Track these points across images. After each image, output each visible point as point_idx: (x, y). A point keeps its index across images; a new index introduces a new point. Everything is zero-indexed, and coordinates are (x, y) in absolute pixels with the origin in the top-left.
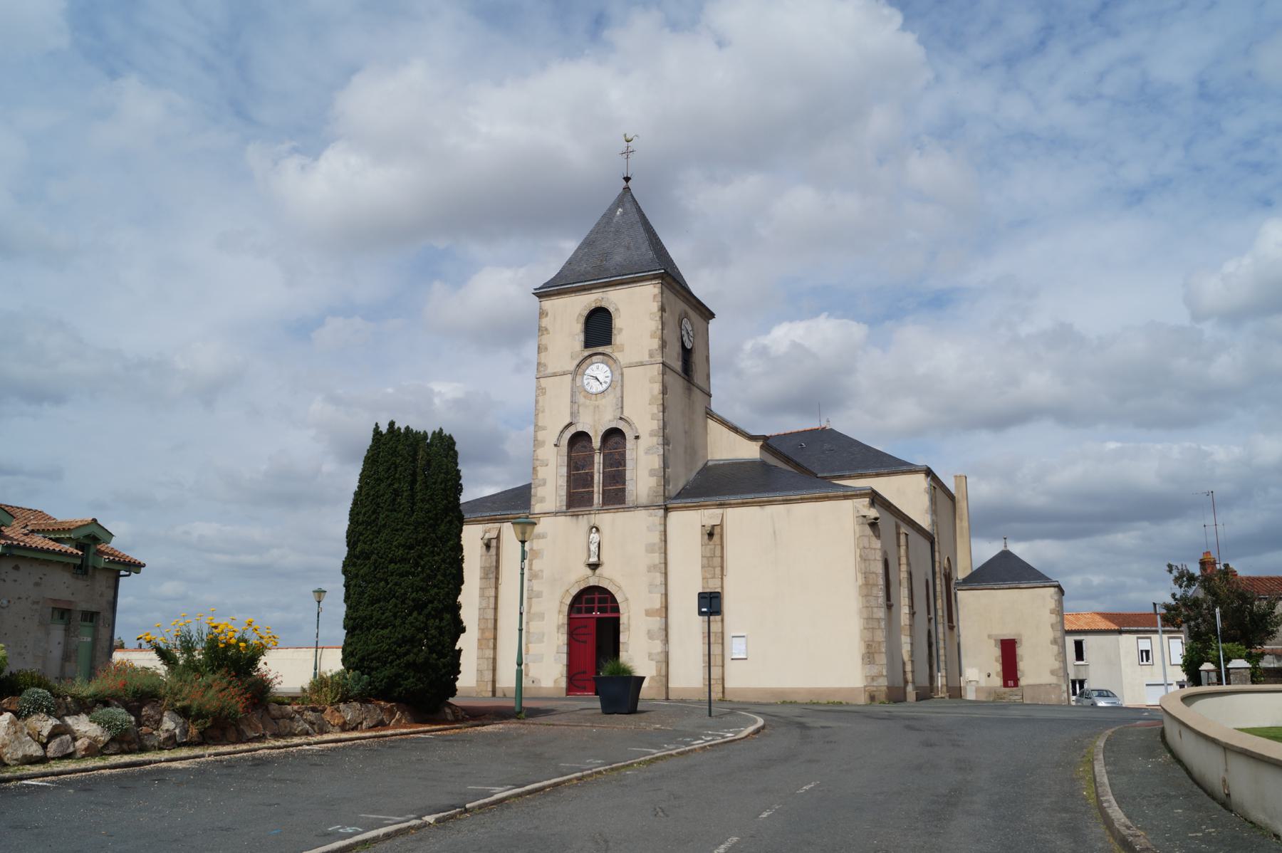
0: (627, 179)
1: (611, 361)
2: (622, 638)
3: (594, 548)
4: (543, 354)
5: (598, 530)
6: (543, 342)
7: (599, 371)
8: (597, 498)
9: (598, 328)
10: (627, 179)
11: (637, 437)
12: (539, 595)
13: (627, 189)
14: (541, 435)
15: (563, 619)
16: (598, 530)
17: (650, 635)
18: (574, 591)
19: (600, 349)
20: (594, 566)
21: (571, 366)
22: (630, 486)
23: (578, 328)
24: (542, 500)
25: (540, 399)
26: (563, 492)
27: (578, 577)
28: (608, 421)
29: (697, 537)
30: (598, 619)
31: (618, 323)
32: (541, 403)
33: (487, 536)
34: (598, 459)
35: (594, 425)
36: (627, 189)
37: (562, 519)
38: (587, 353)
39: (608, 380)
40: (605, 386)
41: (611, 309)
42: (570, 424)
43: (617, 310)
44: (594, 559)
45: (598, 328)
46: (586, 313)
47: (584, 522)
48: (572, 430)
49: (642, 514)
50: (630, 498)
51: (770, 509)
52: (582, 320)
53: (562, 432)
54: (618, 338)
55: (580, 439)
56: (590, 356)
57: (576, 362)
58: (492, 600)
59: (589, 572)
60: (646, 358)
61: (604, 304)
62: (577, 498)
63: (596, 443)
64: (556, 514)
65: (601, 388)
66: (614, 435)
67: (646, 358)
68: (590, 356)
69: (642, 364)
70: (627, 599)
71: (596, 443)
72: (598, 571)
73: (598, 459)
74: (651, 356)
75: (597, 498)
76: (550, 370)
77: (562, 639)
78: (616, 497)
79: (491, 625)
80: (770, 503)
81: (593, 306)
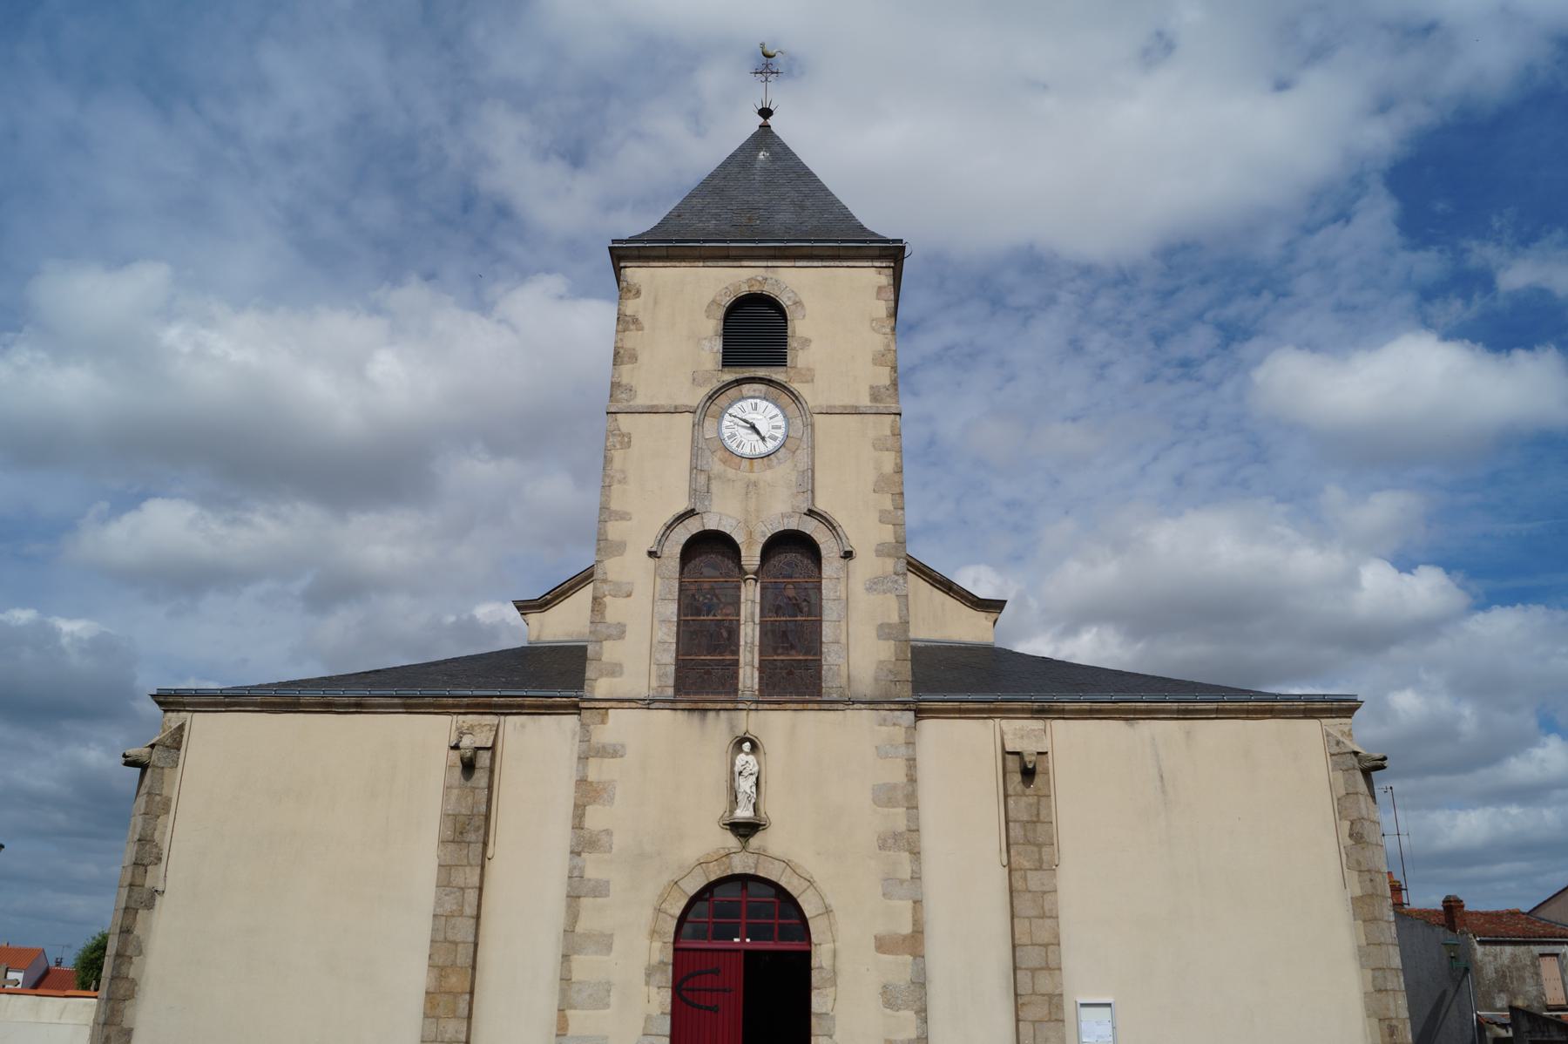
0: (766, 113)
1: (785, 399)
2: (818, 1003)
3: (746, 785)
4: (625, 369)
5: (755, 748)
6: (629, 344)
7: (755, 419)
8: (748, 677)
9: (755, 335)
10: (766, 113)
11: (848, 555)
12: (600, 890)
13: (765, 128)
14: (615, 530)
15: (661, 951)
16: (755, 748)
17: (890, 998)
18: (693, 886)
19: (761, 372)
20: (745, 830)
21: (697, 396)
22: (831, 657)
23: (712, 326)
24: (615, 670)
25: (617, 455)
26: (669, 658)
27: (702, 849)
28: (780, 513)
29: (986, 776)
30: (750, 955)
31: (799, 327)
32: (617, 464)
33: (467, 742)
34: (751, 594)
35: (751, 519)
36: (765, 128)
37: (663, 718)
38: (729, 376)
39: (780, 434)
40: (771, 445)
41: (785, 300)
42: (690, 513)
43: (797, 303)
44: (744, 813)
45: (755, 335)
46: (727, 301)
47: (719, 728)
48: (693, 527)
49: (863, 719)
50: (832, 683)
51: (1148, 729)
52: (721, 313)
53: (670, 527)
54: (799, 357)
55: (710, 546)
56: (739, 382)
57: (704, 391)
58: (472, 895)
59: (732, 841)
60: (865, 401)
61: (768, 289)
62: (701, 675)
63: (751, 557)
64: (649, 703)
65: (762, 449)
66: (793, 546)
67: (865, 401)
68: (739, 382)
69: (856, 412)
70: (828, 911)
71: (751, 557)
72: (755, 841)
73: (751, 594)
74: (875, 397)
75: (748, 677)
76: (641, 401)
77: (661, 999)
78: (796, 675)
79: (463, 958)
80: (1150, 714)
81: (745, 290)
